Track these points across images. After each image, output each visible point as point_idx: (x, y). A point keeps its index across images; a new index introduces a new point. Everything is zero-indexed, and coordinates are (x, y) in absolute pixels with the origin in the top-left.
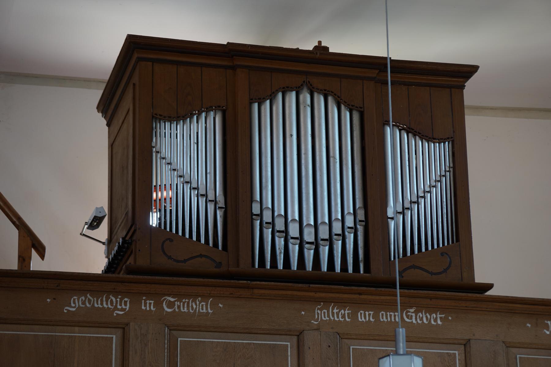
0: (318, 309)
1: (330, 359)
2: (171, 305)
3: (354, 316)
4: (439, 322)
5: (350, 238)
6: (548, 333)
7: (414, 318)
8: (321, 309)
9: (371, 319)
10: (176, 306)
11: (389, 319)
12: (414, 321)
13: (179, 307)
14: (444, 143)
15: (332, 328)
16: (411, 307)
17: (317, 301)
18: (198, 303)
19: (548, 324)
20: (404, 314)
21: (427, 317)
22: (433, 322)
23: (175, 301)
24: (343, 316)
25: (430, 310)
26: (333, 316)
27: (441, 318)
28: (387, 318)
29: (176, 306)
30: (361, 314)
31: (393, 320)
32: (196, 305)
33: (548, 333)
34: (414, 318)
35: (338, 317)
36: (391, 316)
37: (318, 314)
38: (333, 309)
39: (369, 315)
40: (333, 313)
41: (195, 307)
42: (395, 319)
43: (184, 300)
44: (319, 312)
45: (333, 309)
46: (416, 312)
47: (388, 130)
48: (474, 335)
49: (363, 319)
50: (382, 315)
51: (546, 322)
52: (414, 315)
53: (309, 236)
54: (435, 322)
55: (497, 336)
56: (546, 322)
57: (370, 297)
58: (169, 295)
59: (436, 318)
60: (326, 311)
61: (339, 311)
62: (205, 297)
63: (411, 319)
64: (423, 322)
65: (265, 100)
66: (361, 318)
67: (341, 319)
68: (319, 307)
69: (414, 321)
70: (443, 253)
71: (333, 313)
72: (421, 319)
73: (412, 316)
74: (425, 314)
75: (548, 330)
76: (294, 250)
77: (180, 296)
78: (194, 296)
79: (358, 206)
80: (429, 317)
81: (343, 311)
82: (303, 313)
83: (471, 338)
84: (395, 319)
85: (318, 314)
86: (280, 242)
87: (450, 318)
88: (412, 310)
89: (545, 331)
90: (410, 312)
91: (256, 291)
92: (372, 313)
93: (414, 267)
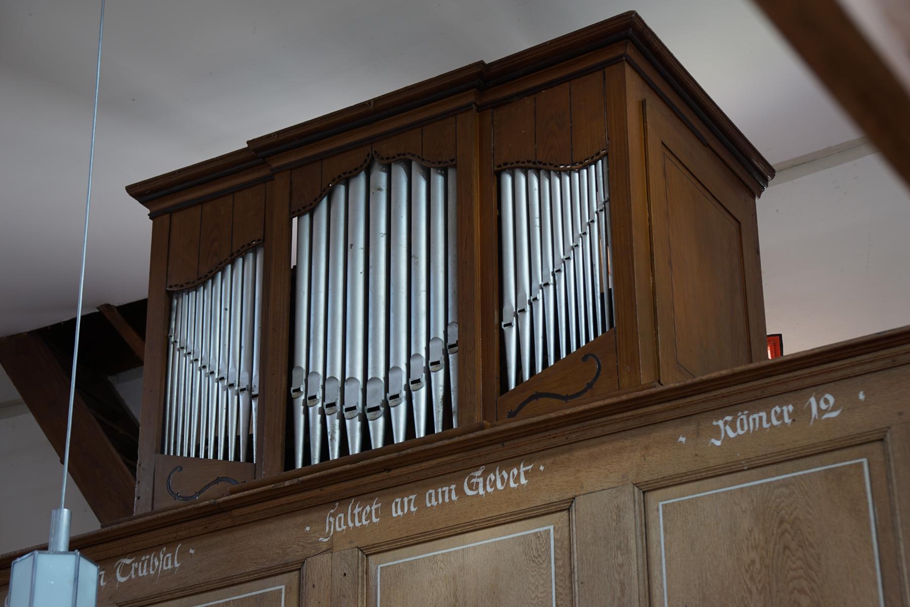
0: (332, 515)
1: (344, 597)
2: (126, 570)
3: (385, 512)
4: (523, 481)
5: (439, 377)
6: (718, 443)
7: (481, 485)
8: (334, 515)
9: (413, 509)
10: (133, 572)
11: (440, 500)
12: (481, 492)
13: (136, 570)
14: (595, 163)
15: (350, 542)
16: (476, 468)
17: (327, 503)
18: (161, 556)
19: (718, 426)
20: (466, 483)
21: (502, 478)
22: (512, 485)
23: (132, 563)
24: (369, 517)
25: (508, 462)
26: (353, 521)
27: (526, 472)
28: (437, 499)
29: (133, 572)
30: (396, 503)
31: (447, 500)
32: (159, 561)
33: (718, 443)
34: (481, 485)
35: (360, 521)
36: (443, 492)
37: (330, 522)
38: (353, 509)
39: (409, 502)
40: (353, 515)
41: (157, 564)
42: (450, 497)
43: (143, 558)
44: (332, 519)
45: (353, 509)
46: (485, 475)
47: (508, 180)
48: (582, 487)
49: (400, 513)
50: (430, 495)
51: (715, 423)
52: (481, 480)
53: (354, 397)
54: (515, 483)
55: (623, 477)
56: (715, 423)
57: (404, 470)
58: (124, 555)
59: (519, 474)
60: (342, 515)
61: (363, 510)
62: (170, 544)
63: (477, 488)
64: (496, 488)
65: (317, 202)
66: (396, 512)
67: (364, 522)
68: (332, 511)
69: (481, 492)
70: (586, 354)
71: (353, 515)
72: (493, 484)
73: (477, 483)
74: (500, 473)
75: (718, 439)
76: (354, 427)
77: (136, 553)
78: (154, 548)
79: (450, 321)
80: (506, 476)
81: (368, 508)
82: (308, 529)
83: (577, 494)
84: (450, 497)
85: (330, 522)
86: (333, 423)
87: (542, 468)
88: (478, 473)
89: (713, 441)
90: (474, 477)
91: (236, 512)
92: (413, 497)
93: (537, 396)
